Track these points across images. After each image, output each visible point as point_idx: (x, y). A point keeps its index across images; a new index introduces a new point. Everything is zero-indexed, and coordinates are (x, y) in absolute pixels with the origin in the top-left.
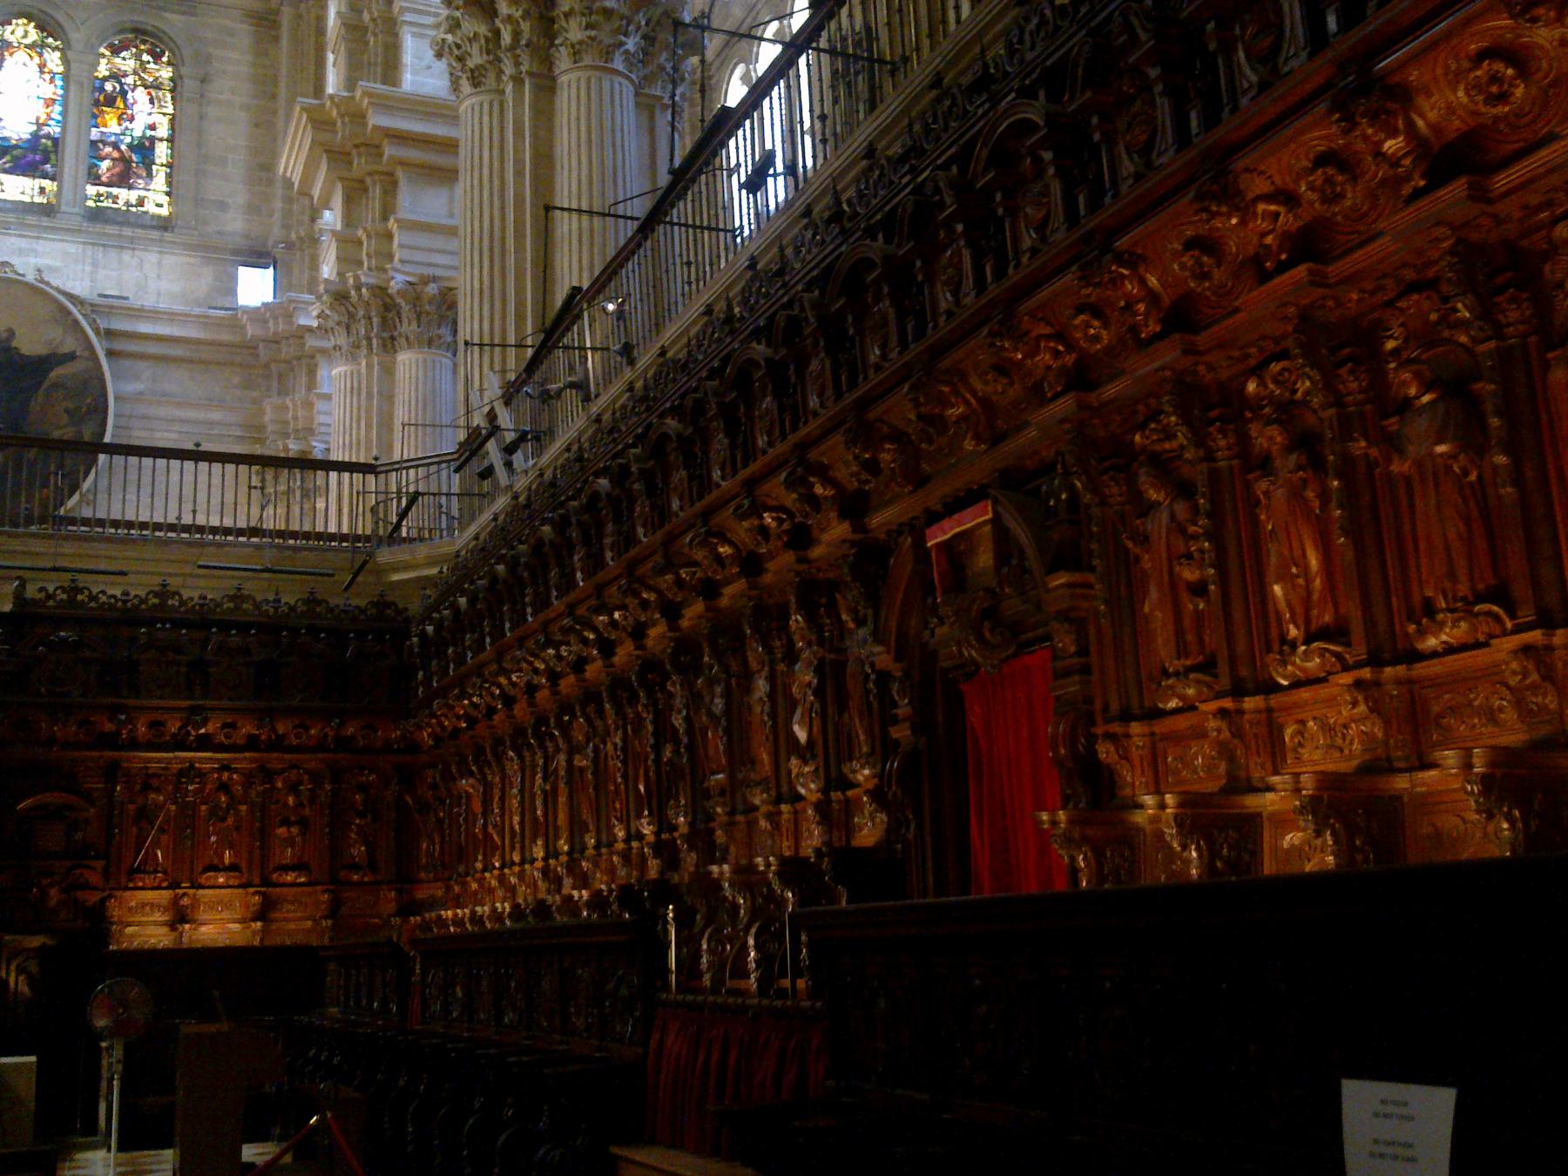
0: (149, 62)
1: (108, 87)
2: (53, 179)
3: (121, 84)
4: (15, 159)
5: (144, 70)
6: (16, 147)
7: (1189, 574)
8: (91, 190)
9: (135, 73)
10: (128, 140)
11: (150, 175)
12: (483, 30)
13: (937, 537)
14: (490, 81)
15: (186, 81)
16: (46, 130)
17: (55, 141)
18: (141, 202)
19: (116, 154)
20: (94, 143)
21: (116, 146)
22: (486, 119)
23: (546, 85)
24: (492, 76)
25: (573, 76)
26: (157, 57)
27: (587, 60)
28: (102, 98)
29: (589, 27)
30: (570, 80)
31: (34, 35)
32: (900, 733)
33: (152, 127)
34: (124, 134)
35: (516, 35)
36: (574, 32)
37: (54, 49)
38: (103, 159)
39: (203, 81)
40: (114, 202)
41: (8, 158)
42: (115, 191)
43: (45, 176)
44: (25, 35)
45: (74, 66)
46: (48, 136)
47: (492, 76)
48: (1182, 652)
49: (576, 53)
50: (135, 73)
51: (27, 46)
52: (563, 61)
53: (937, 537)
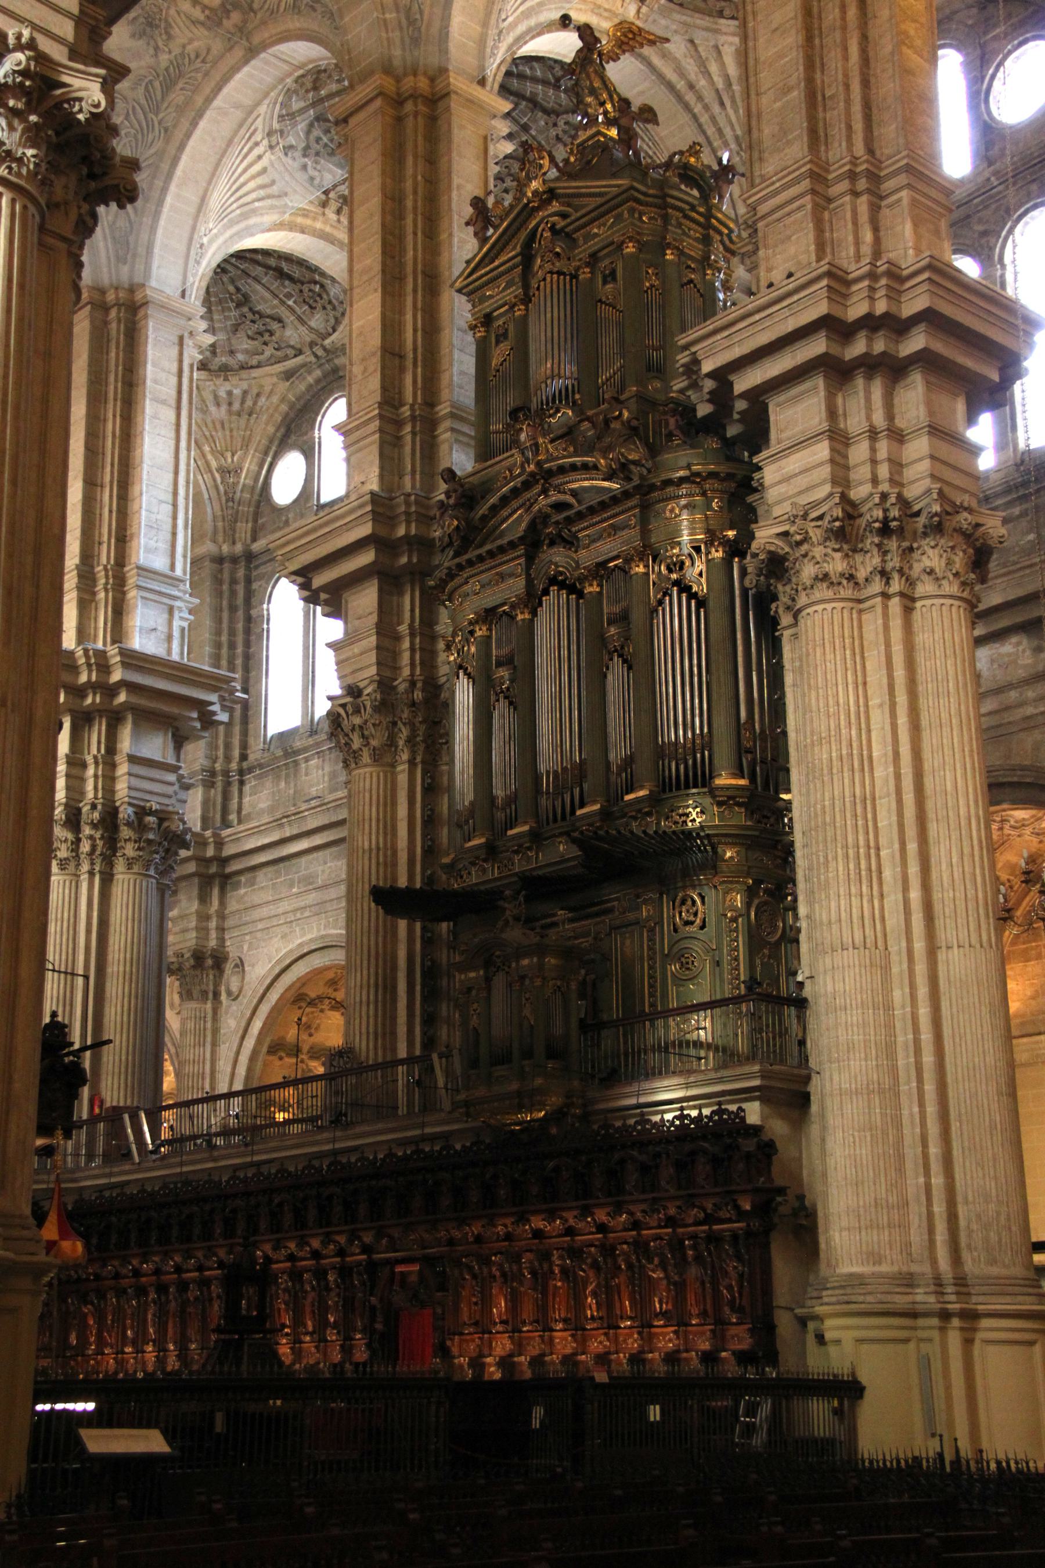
7: (474, 1300)
12: (70, 836)
13: (399, 1269)
14: (71, 868)
22: (67, 891)
23: (107, 879)
24: (73, 864)
25: (127, 877)
27: (136, 869)
29: (139, 849)
30: (124, 881)
32: (379, 1326)
35: (94, 848)
36: (130, 850)
47: (73, 864)
48: (470, 1318)
49: (129, 866)
52: (120, 866)
53: (399, 1269)
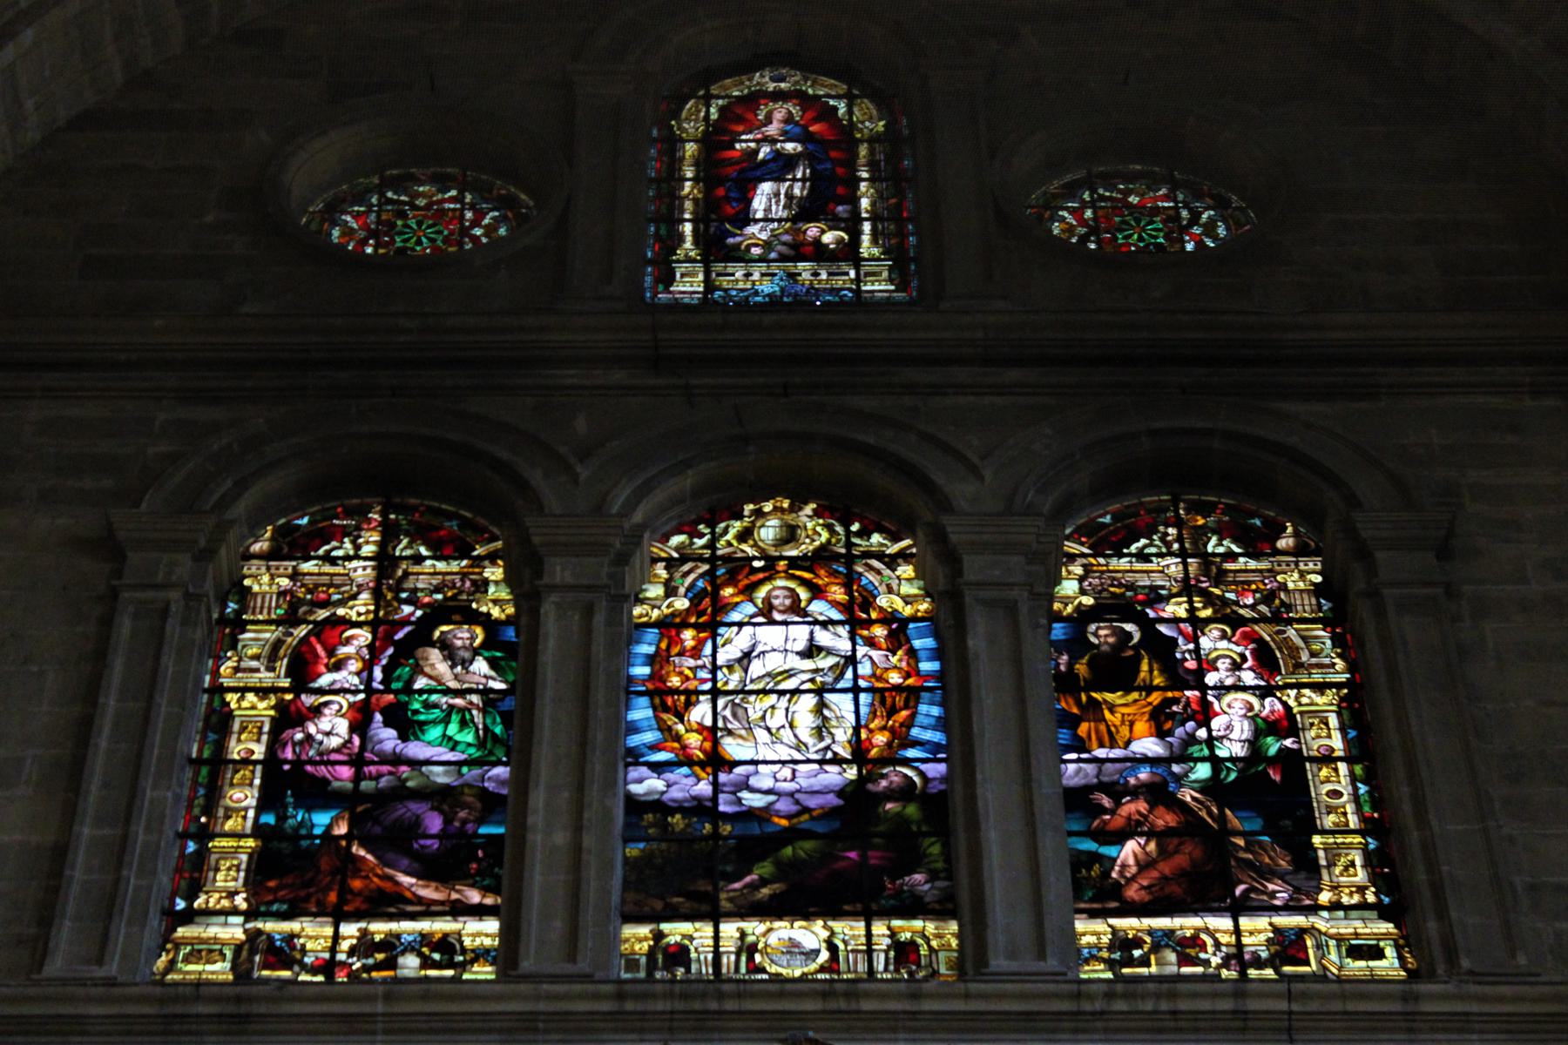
0: (1231, 556)
1: (1100, 634)
2: (940, 912)
3: (1147, 625)
4: (785, 870)
5: (1220, 578)
6: (792, 835)
8: (1092, 931)
9: (1187, 588)
10: (1203, 771)
11: (1307, 868)
15: (1380, 556)
16: (894, 775)
17: (933, 802)
18: (1288, 947)
19: (1165, 819)
20: (1078, 800)
21: (1159, 793)
26: (1258, 543)
28: (1081, 668)
31: (815, 531)
33: (1286, 724)
34: (1183, 758)
37: (892, 562)
38: (1120, 838)
39: (1444, 552)
40: (1184, 960)
41: (764, 869)
42: (1186, 924)
43: (912, 907)
44: (790, 535)
45: (974, 566)
46: (906, 791)
50: (1187, 588)
51: (794, 562)
